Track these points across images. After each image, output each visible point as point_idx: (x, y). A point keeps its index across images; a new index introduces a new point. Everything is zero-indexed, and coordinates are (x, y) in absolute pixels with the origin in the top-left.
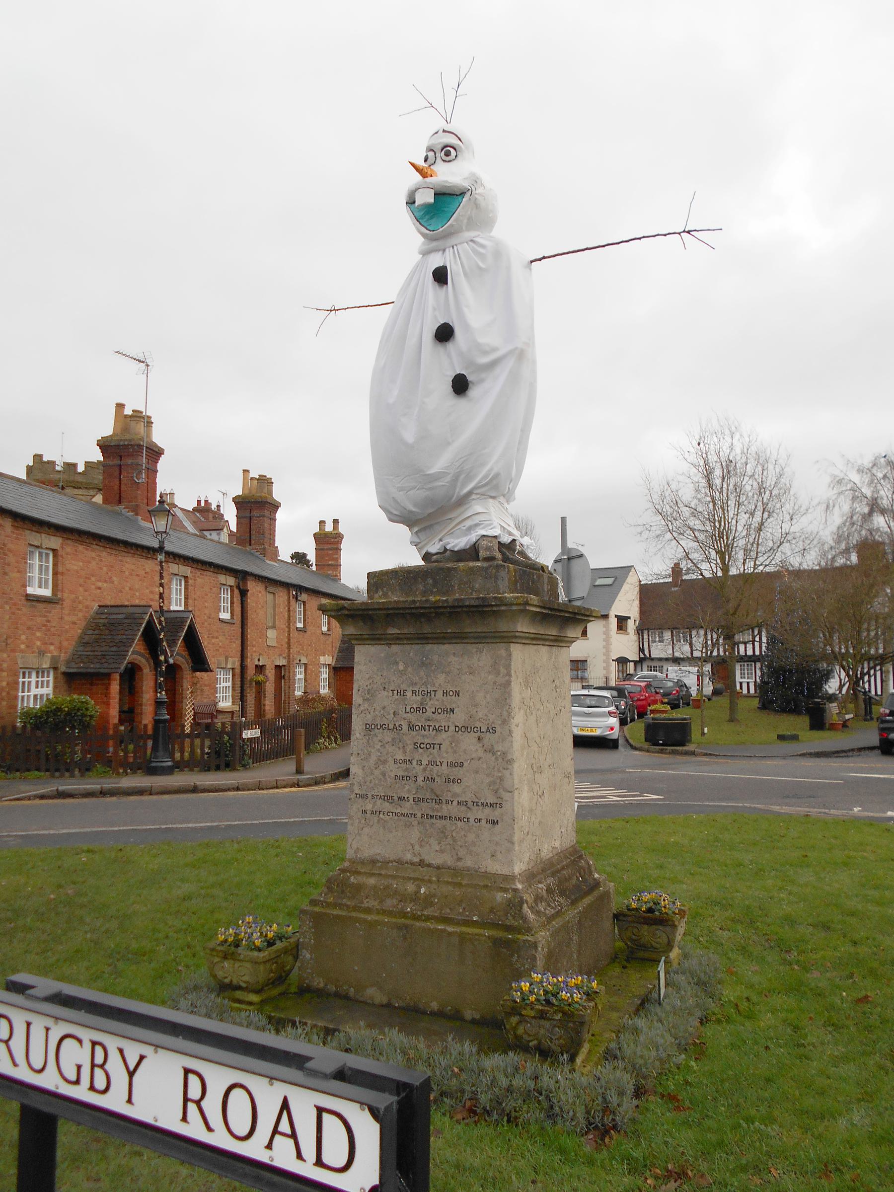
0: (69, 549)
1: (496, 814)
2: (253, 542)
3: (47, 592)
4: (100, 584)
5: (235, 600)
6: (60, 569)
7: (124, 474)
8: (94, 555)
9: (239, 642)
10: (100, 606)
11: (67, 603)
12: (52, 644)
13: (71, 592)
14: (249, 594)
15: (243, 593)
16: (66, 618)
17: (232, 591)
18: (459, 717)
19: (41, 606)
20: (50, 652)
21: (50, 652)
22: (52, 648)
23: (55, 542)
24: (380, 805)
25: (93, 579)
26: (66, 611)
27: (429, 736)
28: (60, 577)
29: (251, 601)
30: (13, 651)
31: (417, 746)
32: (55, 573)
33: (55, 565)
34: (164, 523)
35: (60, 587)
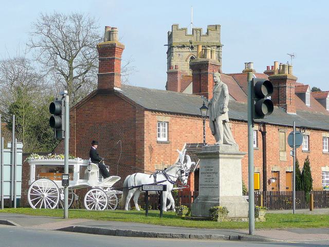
0: (173, 121)
1: (217, 186)
2: (280, 102)
3: (165, 139)
4: (186, 135)
5: (259, 137)
6: (170, 130)
7: (202, 78)
8: (184, 122)
9: (262, 159)
10: (187, 144)
11: (173, 144)
12: (167, 160)
13: (175, 139)
14: (267, 134)
15: (264, 134)
16: (173, 150)
17: (257, 133)
18: (213, 171)
19: (163, 145)
20: (167, 163)
21: (167, 163)
22: (167, 162)
23: (168, 118)
24: (203, 186)
25: (184, 133)
26: (173, 147)
27: (209, 174)
28: (170, 133)
29: (268, 138)
30: (153, 163)
31: (208, 176)
32: (168, 131)
33: (168, 128)
34: (205, 112)
35: (170, 137)
